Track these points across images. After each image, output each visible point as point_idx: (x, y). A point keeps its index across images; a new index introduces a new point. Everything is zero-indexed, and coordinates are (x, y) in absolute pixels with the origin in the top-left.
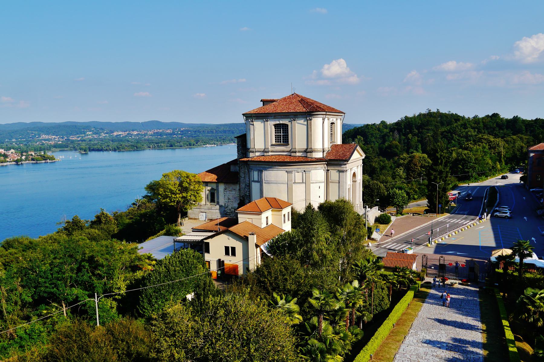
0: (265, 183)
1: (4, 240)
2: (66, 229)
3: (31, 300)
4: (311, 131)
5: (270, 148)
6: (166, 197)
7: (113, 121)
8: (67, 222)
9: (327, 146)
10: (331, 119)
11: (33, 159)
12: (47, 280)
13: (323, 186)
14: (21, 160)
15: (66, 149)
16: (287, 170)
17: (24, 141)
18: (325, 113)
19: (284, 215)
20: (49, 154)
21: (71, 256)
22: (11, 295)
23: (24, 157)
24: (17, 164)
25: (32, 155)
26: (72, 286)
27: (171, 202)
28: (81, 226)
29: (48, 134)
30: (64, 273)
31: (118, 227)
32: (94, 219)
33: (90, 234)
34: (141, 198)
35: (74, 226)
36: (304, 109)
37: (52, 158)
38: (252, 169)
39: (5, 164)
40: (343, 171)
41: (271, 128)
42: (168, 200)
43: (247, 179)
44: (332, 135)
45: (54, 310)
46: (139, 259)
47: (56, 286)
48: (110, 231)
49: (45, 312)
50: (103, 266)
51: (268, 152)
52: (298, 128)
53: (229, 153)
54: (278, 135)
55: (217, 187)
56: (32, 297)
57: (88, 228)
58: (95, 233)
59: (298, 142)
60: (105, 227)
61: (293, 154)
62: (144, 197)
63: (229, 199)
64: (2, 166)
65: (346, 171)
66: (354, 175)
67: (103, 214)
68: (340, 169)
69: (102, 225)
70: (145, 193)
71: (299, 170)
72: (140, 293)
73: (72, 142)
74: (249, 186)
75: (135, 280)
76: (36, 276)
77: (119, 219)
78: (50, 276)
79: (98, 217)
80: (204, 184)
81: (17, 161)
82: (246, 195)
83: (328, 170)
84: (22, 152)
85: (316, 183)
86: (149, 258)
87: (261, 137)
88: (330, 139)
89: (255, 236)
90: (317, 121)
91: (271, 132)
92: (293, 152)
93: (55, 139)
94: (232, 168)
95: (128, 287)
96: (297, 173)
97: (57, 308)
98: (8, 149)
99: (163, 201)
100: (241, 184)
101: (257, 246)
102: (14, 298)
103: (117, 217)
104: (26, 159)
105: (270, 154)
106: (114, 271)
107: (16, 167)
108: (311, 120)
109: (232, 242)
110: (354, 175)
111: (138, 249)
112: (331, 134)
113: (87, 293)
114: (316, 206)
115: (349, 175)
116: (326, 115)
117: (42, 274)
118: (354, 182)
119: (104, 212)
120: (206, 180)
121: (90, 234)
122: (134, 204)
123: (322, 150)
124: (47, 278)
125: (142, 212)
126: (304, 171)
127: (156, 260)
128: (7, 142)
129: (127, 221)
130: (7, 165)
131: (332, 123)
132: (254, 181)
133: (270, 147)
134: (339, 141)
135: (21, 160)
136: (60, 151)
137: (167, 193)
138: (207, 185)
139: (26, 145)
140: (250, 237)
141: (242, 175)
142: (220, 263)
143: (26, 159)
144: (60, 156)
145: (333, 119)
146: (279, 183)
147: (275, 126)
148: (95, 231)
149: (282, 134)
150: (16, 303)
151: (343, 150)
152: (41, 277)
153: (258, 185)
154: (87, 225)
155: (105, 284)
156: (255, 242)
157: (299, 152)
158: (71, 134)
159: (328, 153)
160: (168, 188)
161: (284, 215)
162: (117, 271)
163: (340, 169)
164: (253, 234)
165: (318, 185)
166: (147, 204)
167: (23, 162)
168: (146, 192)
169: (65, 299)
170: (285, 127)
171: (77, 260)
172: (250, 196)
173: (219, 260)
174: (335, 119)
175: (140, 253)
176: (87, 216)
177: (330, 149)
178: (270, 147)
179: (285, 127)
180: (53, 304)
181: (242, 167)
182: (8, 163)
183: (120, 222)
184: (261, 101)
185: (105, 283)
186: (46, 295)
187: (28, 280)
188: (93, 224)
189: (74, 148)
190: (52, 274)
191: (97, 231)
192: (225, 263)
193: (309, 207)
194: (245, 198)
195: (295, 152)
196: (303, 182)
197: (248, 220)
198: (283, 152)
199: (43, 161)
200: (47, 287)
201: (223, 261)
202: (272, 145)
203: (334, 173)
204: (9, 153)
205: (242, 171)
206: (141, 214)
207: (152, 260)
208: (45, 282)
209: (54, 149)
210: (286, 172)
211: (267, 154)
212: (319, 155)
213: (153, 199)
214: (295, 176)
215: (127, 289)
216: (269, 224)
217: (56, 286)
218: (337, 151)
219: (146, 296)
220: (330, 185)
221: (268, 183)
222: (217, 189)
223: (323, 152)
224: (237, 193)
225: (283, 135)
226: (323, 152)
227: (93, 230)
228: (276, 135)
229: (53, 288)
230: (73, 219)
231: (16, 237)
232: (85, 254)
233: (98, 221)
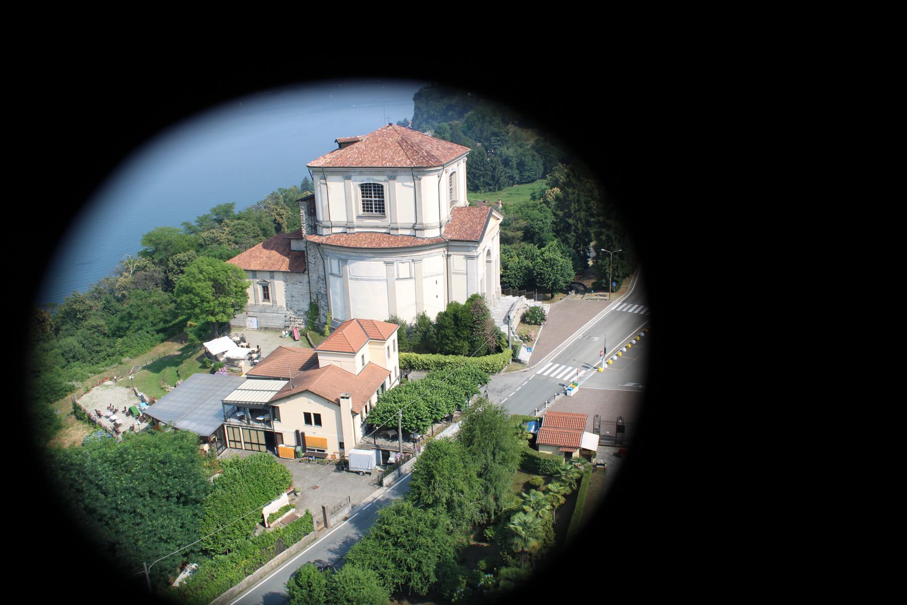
0: (351, 279)
4: (420, 196)
5: (356, 222)
9: (446, 215)
13: (442, 280)
36: (408, 162)
38: (327, 256)
40: (472, 258)
41: (356, 190)
43: (321, 269)
51: (353, 228)
52: (399, 194)
61: (392, 232)
65: (477, 257)
66: (489, 253)
68: (467, 253)
71: (404, 259)
80: (251, 274)
82: (320, 293)
83: (448, 256)
85: (431, 276)
90: (429, 182)
91: (356, 195)
92: (392, 229)
96: (402, 265)
100: (311, 274)
101: (354, 414)
105: (356, 230)
108: (420, 179)
109: (314, 407)
110: (489, 253)
114: (433, 317)
115: (483, 258)
118: (489, 262)
132: (332, 274)
133: (355, 220)
134: (462, 198)
138: (255, 277)
142: (300, 438)
147: (362, 186)
151: (470, 219)
157: (402, 228)
159: (448, 226)
163: (467, 253)
165: (435, 279)
170: (379, 190)
173: (297, 432)
178: (355, 220)
184: (336, 141)
192: (306, 435)
193: (423, 319)
194: (320, 297)
197: (334, 363)
198: (377, 227)
201: (303, 434)
202: (358, 217)
203: (458, 259)
211: (352, 231)
212: (433, 233)
218: (462, 222)
220: (454, 278)
221: (356, 279)
223: (441, 227)
224: (306, 286)
225: (374, 199)
226: (441, 227)
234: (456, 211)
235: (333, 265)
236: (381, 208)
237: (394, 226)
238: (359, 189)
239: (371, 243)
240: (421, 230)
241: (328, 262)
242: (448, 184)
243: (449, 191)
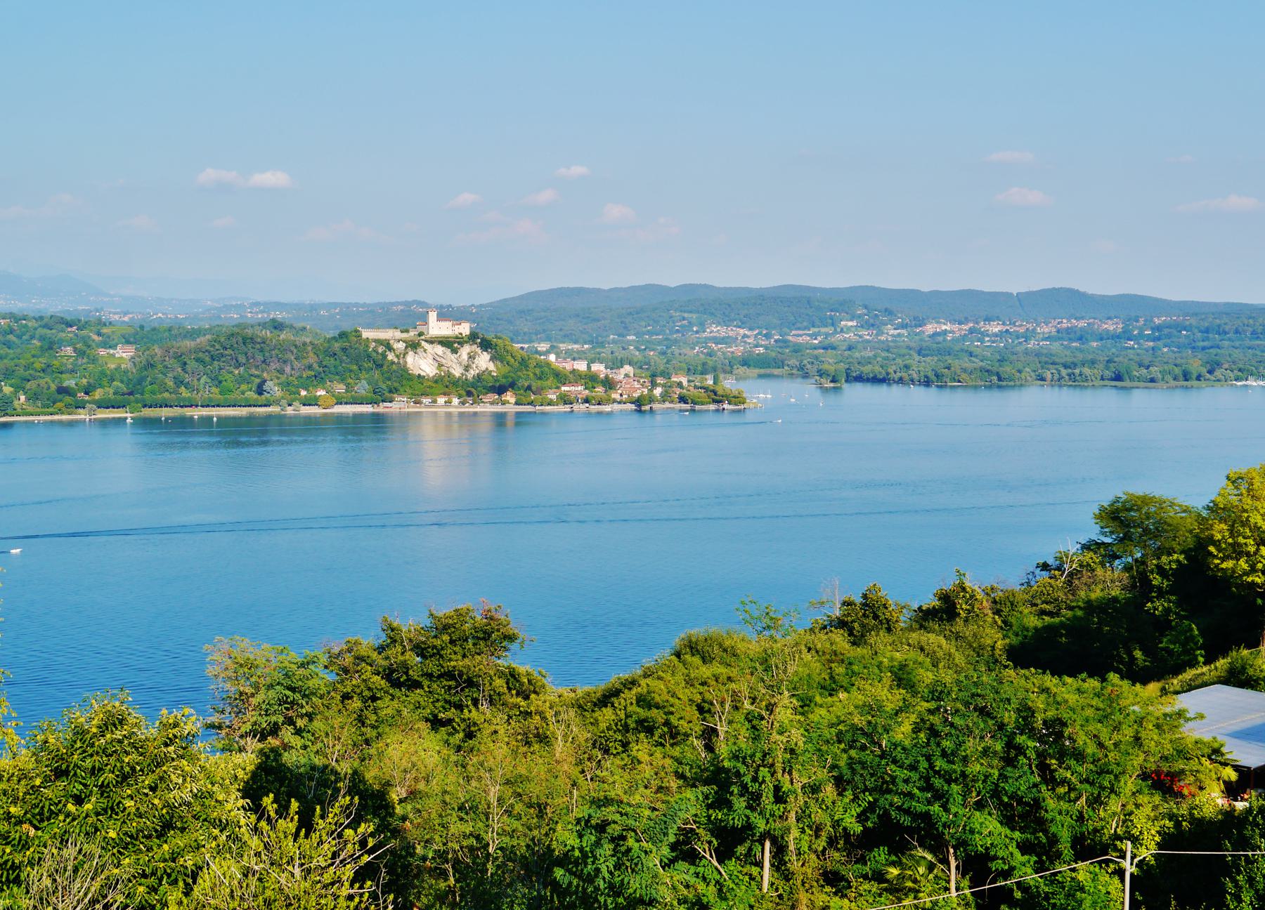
1: (683, 635)
2: (842, 624)
3: (859, 829)
6: (1237, 551)
7: (987, 288)
8: (845, 603)
11: (683, 399)
12: (914, 776)
14: (651, 400)
15: (776, 371)
17: (660, 343)
20: (728, 384)
21: (983, 712)
22: (812, 803)
23: (658, 391)
24: (640, 411)
25: (680, 385)
26: (980, 806)
27: (1253, 570)
28: (888, 621)
29: (726, 322)
30: (965, 760)
31: (1005, 637)
32: (930, 601)
33: (922, 649)
34: (1073, 548)
35: (863, 619)
37: (737, 399)
39: (607, 408)
42: (1243, 564)
45: (922, 870)
46: (1182, 754)
47: (941, 797)
48: (982, 647)
49: (894, 871)
50: (1080, 756)
56: (861, 818)
57: (911, 629)
58: (940, 646)
60: (968, 632)
62: (1085, 547)
64: (600, 413)
67: (964, 589)
69: (959, 625)
70: (1093, 532)
72: (1229, 869)
73: (797, 349)
75: (1193, 820)
76: (882, 757)
77: (1006, 610)
78: (924, 765)
79: (946, 598)
81: (638, 402)
84: (654, 376)
86: (1215, 753)
93: (746, 339)
95: (1167, 841)
97: (931, 867)
98: (616, 364)
99: (1224, 566)
102: (819, 816)
103: (1002, 606)
104: (665, 397)
106: (1116, 776)
107: (636, 416)
111: (1187, 720)
113: (1017, 835)
117: (899, 754)
119: (967, 584)
121: (922, 649)
122: (1045, 567)
124: (913, 768)
125: (1093, 596)
127: (1237, 768)
128: (614, 342)
129: (1033, 622)
130: (610, 414)
135: (651, 400)
136: (760, 376)
137: (1241, 540)
139: (664, 353)
143: (665, 397)
144: (760, 394)
148: (934, 639)
150: (818, 830)
152: (895, 762)
154: (904, 619)
155: (1081, 818)
158: (793, 325)
160: (1245, 524)
162: (1129, 784)
166: (1099, 571)
167: (656, 406)
168: (1097, 528)
169: (961, 844)
171: (1001, 726)
175: (1192, 732)
176: (911, 591)
180: (920, 852)
182: (616, 407)
183: (1013, 620)
185: (1081, 813)
186: (906, 821)
187: (858, 767)
188: (925, 617)
189: (801, 368)
190: (928, 758)
191: (943, 642)
199: (712, 407)
200: (910, 795)
204: (619, 375)
206: (1089, 603)
207: (1225, 764)
208: (906, 781)
209: (742, 370)
213: (1115, 557)
215: (1160, 846)
217: (941, 797)
219: (1251, 881)
227: (932, 637)
229: (929, 803)
230: (865, 596)
231: (714, 630)
232: (1032, 712)
233: (945, 611)
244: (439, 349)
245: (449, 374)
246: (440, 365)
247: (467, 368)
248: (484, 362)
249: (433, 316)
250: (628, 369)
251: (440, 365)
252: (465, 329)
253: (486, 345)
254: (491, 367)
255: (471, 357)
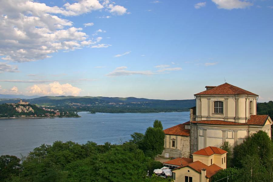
0: (208, 137)
10: (250, 100)
16: (222, 129)
18: (247, 95)
19: (222, 159)
41: (212, 103)
43: (196, 134)
44: (251, 109)
53: (185, 117)
54: (216, 108)
55: (177, 138)
59: (230, 112)
63: (183, 146)
71: (230, 130)
74: (197, 138)
87: (205, 109)
88: (249, 112)
89: (206, 171)
90: (242, 100)
91: (212, 106)
92: (226, 119)
94: (187, 127)
100: (191, 137)
112: (250, 108)
116: (248, 96)
120: (170, 133)
123: (245, 118)
126: (234, 131)
131: (251, 102)
132: (200, 136)
134: (255, 113)
140: (202, 172)
141: (192, 131)
145: (251, 99)
146: (217, 138)
149: (219, 107)
153: (203, 138)
156: (206, 175)
157: (230, 119)
161: (222, 159)
164: (204, 170)
172: (197, 145)
174: (252, 99)
177: (250, 118)
178: (211, 115)
179: (221, 103)
181: (193, 126)
195: (228, 119)
196: (232, 138)
198: (220, 118)
204: (56, 111)
205: (193, 129)
210: (222, 131)
212: (243, 121)
214: (227, 134)
216: (213, 164)
221: (210, 137)
222: (177, 140)
225: (219, 107)
226: (246, 120)
228: (215, 108)
234: (252, 116)
235: (201, 132)
236: (221, 112)
237: (227, 118)
238: (214, 102)
239: (217, 123)
240: (237, 119)
241: (199, 131)
242: (249, 106)
243: (249, 108)
244: (22, 107)
245: (24, 112)
246: (22, 110)
247: (28, 110)
248: (31, 109)
249: (21, 101)
250: (58, 110)
251: (22, 110)
252: (27, 103)
253: (31, 106)
254: (33, 110)
255: (29, 108)
